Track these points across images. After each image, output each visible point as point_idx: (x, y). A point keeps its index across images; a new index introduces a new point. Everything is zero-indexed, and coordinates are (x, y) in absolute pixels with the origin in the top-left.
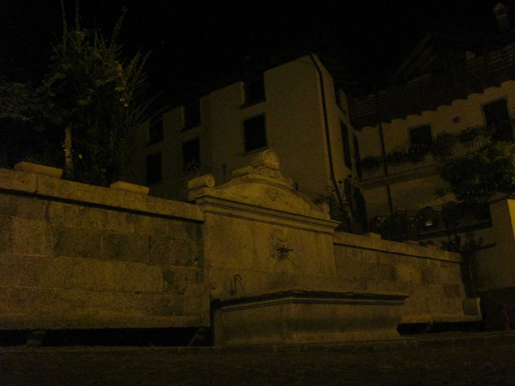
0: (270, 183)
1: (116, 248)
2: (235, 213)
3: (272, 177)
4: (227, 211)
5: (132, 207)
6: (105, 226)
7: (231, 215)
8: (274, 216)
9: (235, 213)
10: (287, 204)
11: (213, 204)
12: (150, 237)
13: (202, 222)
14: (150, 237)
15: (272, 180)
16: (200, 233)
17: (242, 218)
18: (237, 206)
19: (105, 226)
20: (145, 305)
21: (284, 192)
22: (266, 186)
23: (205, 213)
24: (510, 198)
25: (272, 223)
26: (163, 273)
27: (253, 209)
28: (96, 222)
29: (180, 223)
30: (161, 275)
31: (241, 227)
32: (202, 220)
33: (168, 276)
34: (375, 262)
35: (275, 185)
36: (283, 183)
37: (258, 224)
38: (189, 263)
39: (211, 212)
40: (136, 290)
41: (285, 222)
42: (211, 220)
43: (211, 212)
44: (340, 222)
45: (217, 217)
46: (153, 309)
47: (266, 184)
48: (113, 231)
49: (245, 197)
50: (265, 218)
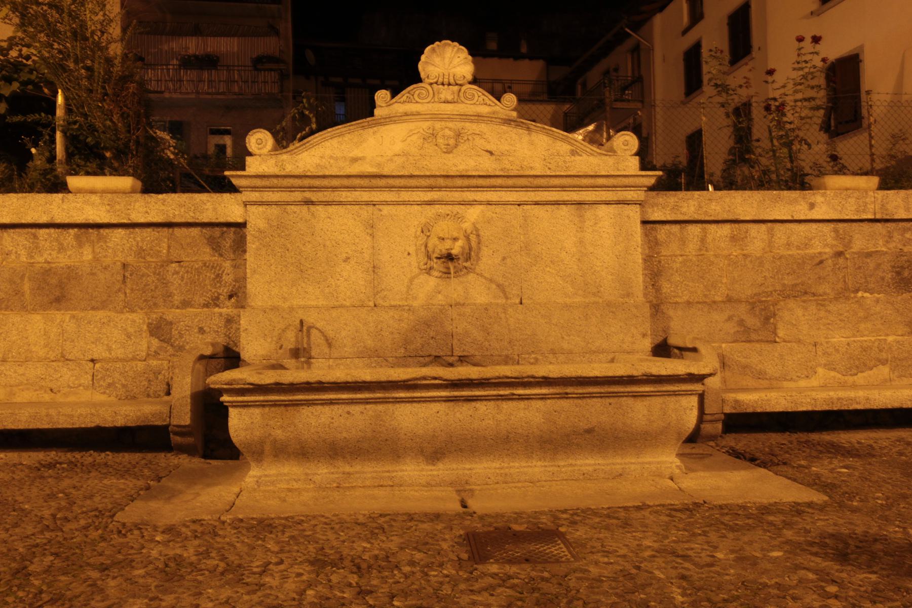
0: (436, 117)
1: (56, 291)
2: (313, 196)
3: (447, 102)
4: (298, 196)
5: (79, 219)
6: (32, 257)
7: (309, 203)
8: (431, 188)
9: (313, 196)
10: (491, 153)
11: (254, 188)
12: (124, 266)
13: (243, 225)
14: (124, 266)
15: (449, 108)
16: (240, 246)
17: (340, 203)
18: (317, 182)
19: (32, 257)
20: (109, 380)
21: (483, 127)
22: (426, 125)
23: (246, 205)
24: (71, 175)
25: (430, 203)
26: (149, 325)
27: (365, 182)
28: (16, 253)
29: (195, 231)
30: (145, 327)
31: (338, 224)
32: (240, 220)
33: (158, 329)
34: (827, 250)
35: (464, 117)
36: (484, 110)
37: (386, 210)
38: (215, 302)
39: (255, 203)
40: (90, 357)
41: (470, 196)
42: (257, 218)
43: (255, 203)
44: (660, 173)
45: (274, 211)
46: (124, 386)
47: (426, 120)
48: (49, 263)
49: (355, 160)
50: (405, 196)
